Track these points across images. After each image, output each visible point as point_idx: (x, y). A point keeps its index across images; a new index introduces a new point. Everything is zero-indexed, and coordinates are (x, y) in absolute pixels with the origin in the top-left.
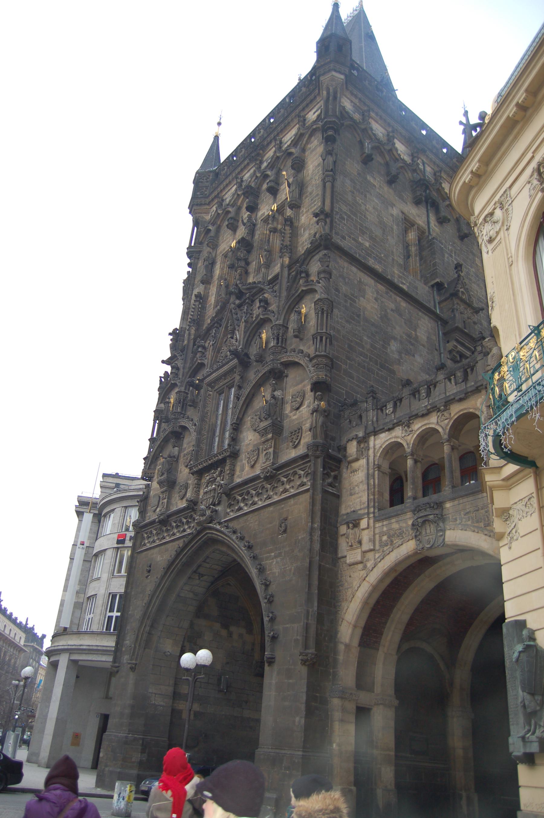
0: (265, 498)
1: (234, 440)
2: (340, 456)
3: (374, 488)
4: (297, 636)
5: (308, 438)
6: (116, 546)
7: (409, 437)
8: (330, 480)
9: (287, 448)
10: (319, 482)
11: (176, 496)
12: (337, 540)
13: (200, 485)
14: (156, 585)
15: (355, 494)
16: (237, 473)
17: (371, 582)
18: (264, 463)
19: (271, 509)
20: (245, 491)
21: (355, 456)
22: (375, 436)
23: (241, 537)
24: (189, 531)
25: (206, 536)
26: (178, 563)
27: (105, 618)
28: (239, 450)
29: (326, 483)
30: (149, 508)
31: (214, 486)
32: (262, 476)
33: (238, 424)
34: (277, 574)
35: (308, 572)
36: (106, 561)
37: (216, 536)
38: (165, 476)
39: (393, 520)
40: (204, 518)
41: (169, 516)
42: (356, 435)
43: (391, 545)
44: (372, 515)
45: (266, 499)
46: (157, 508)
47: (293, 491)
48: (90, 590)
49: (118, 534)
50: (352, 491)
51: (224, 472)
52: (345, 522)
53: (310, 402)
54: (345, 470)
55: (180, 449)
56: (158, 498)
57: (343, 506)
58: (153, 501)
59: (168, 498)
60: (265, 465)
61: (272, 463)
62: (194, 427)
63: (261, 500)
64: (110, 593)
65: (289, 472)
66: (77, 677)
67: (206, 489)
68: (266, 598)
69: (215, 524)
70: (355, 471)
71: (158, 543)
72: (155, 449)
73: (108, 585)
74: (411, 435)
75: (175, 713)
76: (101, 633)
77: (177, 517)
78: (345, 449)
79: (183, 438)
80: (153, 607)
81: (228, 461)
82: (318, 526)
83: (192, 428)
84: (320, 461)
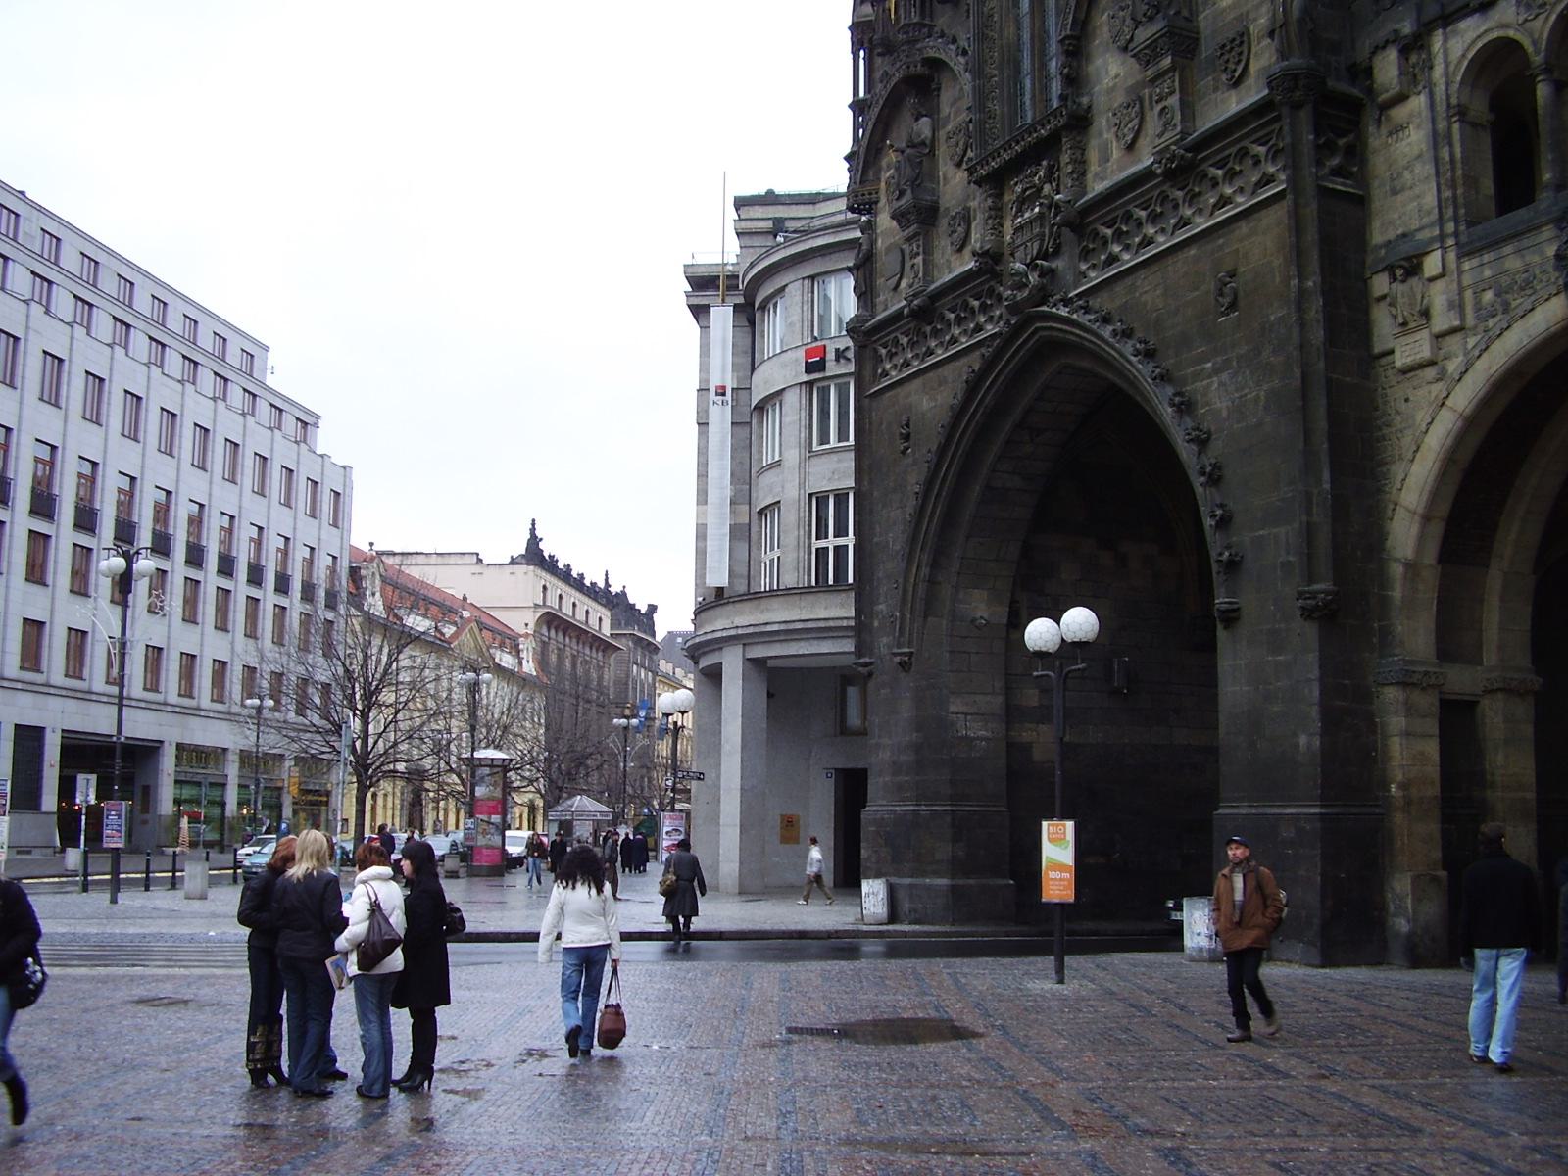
0: (1175, 226)
1: (1075, 81)
2: (1356, 92)
3: (1453, 169)
4: (1288, 553)
5: (1267, 55)
6: (805, 378)
7: (1538, 23)
8: (1335, 161)
9: (1216, 89)
10: (1309, 170)
11: (943, 243)
12: (1367, 312)
13: (1000, 209)
14: (929, 468)
15: (1403, 190)
16: (1094, 168)
17: (1460, 410)
18: (1160, 136)
19: (1192, 251)
20: (1120, 212)
21: (1395, 89)
22: (1445, 26)
23: (1123, 331)
24: (991, 329)
25: (1036, 337)
26: (976, 411)
27: (810, 554)
28: (1089, 107)
29: (1326, 171)
30: (880, 282)
31: (1037, 210)
32: (1159, 171)
33: (1078, 39)
34: (1225, 413)
35: (1300, 403)
36: (786, 420)
37: (1061, 335)
38: (908, 197)
39: (1508, 249)
40: (1026, 293)
42: (1396, 32)
43: (1506, 311)
44: (1451, 242)
45: (1177, 227)
46: (900, 279)
47: (1243, 202)
48: (761, 494)
49: (804, 348)
51: (1058, 170)
52: (1384, 265)
54: (1372, 129)
55: (933, 119)
56: (899, 254)
57: (1376, 224)
58: (886, 263)
59: (924, 252)
60: (1163, 140)
61: (1181, 132)
62: (962, 59)
63: (1163, 230)
64: (811, 495)
65: (1227, 152)
66: (770, 695)
67: (1019, 220)
68: (1203, 474)
69: (1055, 305)
70: (1398, 129)
71: (917, 366)
72: (870, 127)
73: (802, 476)
74: (1542, 17)
75: (1016, 751)
76: (807, 591)
78: (1369, 72)
79: (939, 89)
81: (1064, 140)
82: (1315, 283)
83: (958, 64)
84: (1305, 115)
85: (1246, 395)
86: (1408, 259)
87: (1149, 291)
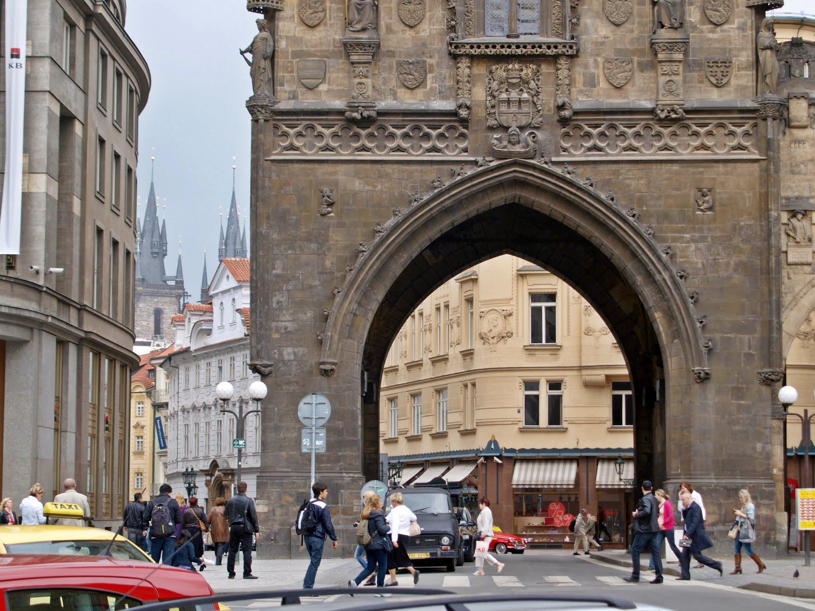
4: (750, 348)
9: (701, 82)
15: (799, 173)
19: (675, 167)
20: (607, 123)
24: (450, 156)
30: (280, 74)
34: (700, 265)
41: (381, 113)
45: (661, 149)
46: (321, 83)
47: (721, 154)
50: (795, 168)
53: (745, 24)
56: (323, 64)
60: (664, 99)
68: (692, 298)
69: (546, 163)
77: (403, 120)
80: (367, 273)
81: (562, 62)
85: (719, 259)
86: (806, 211)
87: (634, 180)
